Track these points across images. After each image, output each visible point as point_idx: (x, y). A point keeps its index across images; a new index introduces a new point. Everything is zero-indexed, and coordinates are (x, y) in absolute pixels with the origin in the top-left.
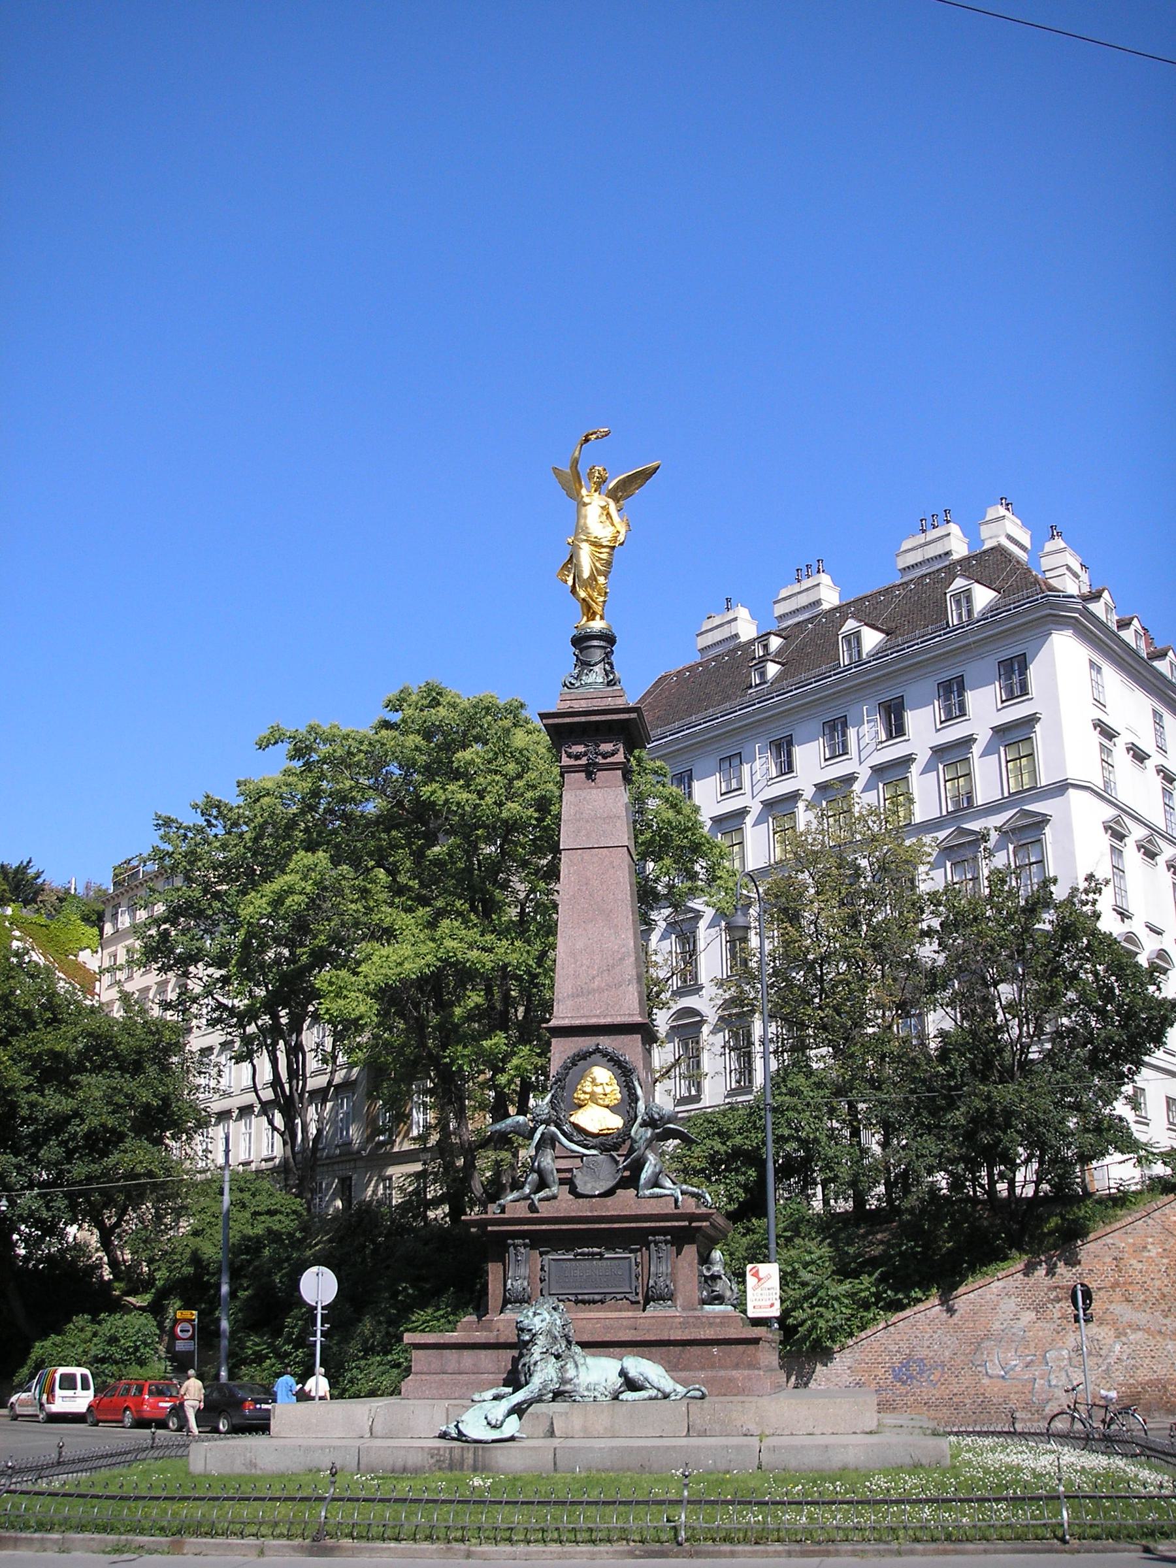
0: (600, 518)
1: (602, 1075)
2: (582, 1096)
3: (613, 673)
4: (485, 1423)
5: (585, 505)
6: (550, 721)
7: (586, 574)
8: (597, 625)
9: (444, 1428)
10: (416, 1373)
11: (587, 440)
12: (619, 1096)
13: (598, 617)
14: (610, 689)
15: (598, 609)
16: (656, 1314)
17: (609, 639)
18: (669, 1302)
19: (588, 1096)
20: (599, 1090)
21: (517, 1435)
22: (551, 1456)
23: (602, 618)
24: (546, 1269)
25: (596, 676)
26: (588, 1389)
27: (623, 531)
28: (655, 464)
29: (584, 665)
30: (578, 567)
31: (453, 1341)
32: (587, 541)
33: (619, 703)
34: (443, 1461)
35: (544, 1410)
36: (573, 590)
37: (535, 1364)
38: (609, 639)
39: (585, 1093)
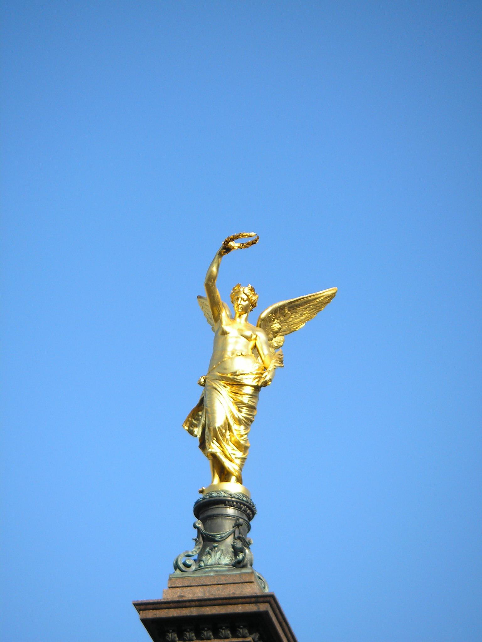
0: (245, 350)
3: (242, 551)
5: (224, 333)
6: (151, 614)
7: (219, 422)
8: (233, 488)
11: (227, 249)
13: (233, 479)
14: (237, 572)
15: (232, 466)
17: (247, 509)
23: (239, 480)
25: (221, 557)
27: (272, 364)
28: (329, 292)
29: (207, 540)
30: (210, 415)
32: (223, 378)
33: (249, 590)
36: (203, 445)
38: (247, 509)
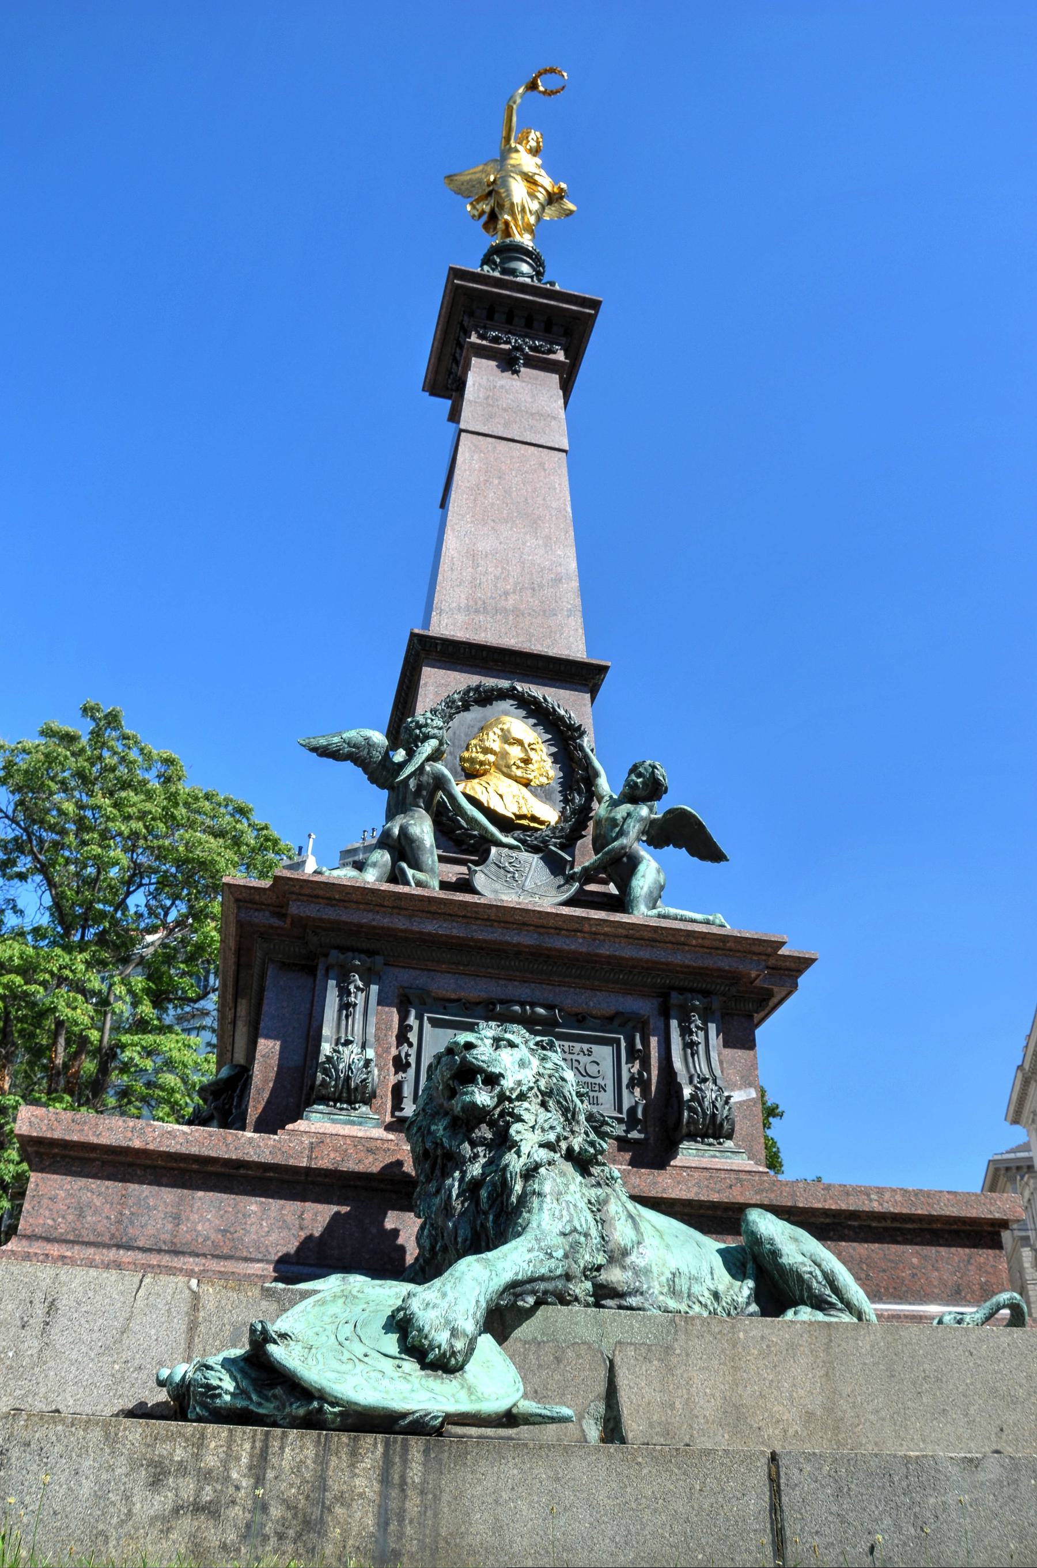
1: (521, 728)
2: (481, 757)
4: (391, 1343)
9: (181, 1370)
10: (31, 1237)
12: (552, 773)
16: (705, 1162)
18: (729, 1144)
19: (491, 758)
20: (515, 753)
21: (529, 1406)
22: (757, 1501)
24: (413, 1037)
26: (673, 1292)
31: (173, 1146)
34: (211, 1510)
35: (590, 1334)
37: (530, 1173)
39: (486, 751)
